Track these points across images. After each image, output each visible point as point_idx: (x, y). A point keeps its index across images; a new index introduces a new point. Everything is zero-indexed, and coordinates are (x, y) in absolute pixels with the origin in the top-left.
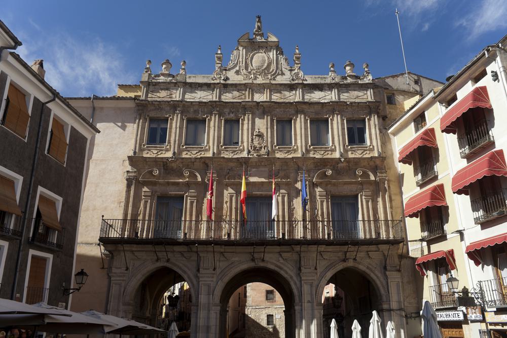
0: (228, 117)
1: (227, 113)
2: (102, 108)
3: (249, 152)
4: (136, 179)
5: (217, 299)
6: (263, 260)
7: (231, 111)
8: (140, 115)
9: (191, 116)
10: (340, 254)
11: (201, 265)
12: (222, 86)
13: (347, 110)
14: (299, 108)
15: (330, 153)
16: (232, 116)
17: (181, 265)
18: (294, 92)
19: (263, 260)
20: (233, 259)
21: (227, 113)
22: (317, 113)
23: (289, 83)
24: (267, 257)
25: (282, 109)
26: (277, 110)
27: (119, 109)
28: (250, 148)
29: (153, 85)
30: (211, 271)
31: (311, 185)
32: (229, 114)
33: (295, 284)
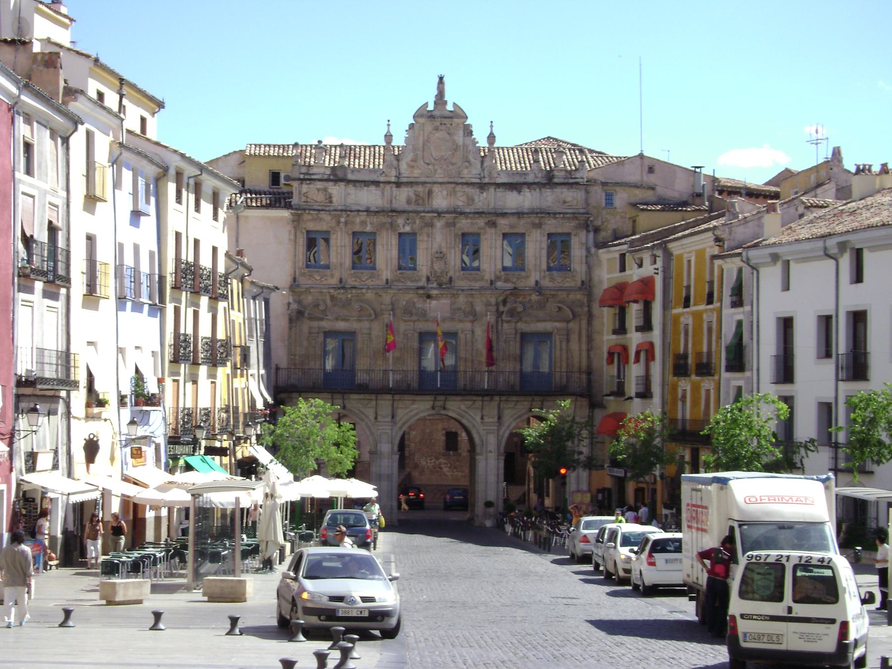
0: (402, 231)
1: (401, 226)
2: (246, 217)
3: (428, 279)
4: (300, 313)
5: (396, 448)
6: (444, 408)
7: (406, 223)
8: (295, 228)
9: (357, 228)
10: (526, 403)
11: (379, 413)
12: (394, 185)
13: (549, 222)
14: (493, 216)
15: (524, 280)
16: (407, 229)
17: (357, 411)
18: (485, 194)
19: (444, 408)
20: (412, 406)
21: (401, 226)
22: (511, 226)
23: (478, 181)
24: (449, 405)
25: (469, 221)
26: (464, 221)
27: (268, 218)
28: (429, 275)
29: (307, 184)
30: (389, 419)
31: (500, 322)
32: (404, 226)
33: (478, 433)
